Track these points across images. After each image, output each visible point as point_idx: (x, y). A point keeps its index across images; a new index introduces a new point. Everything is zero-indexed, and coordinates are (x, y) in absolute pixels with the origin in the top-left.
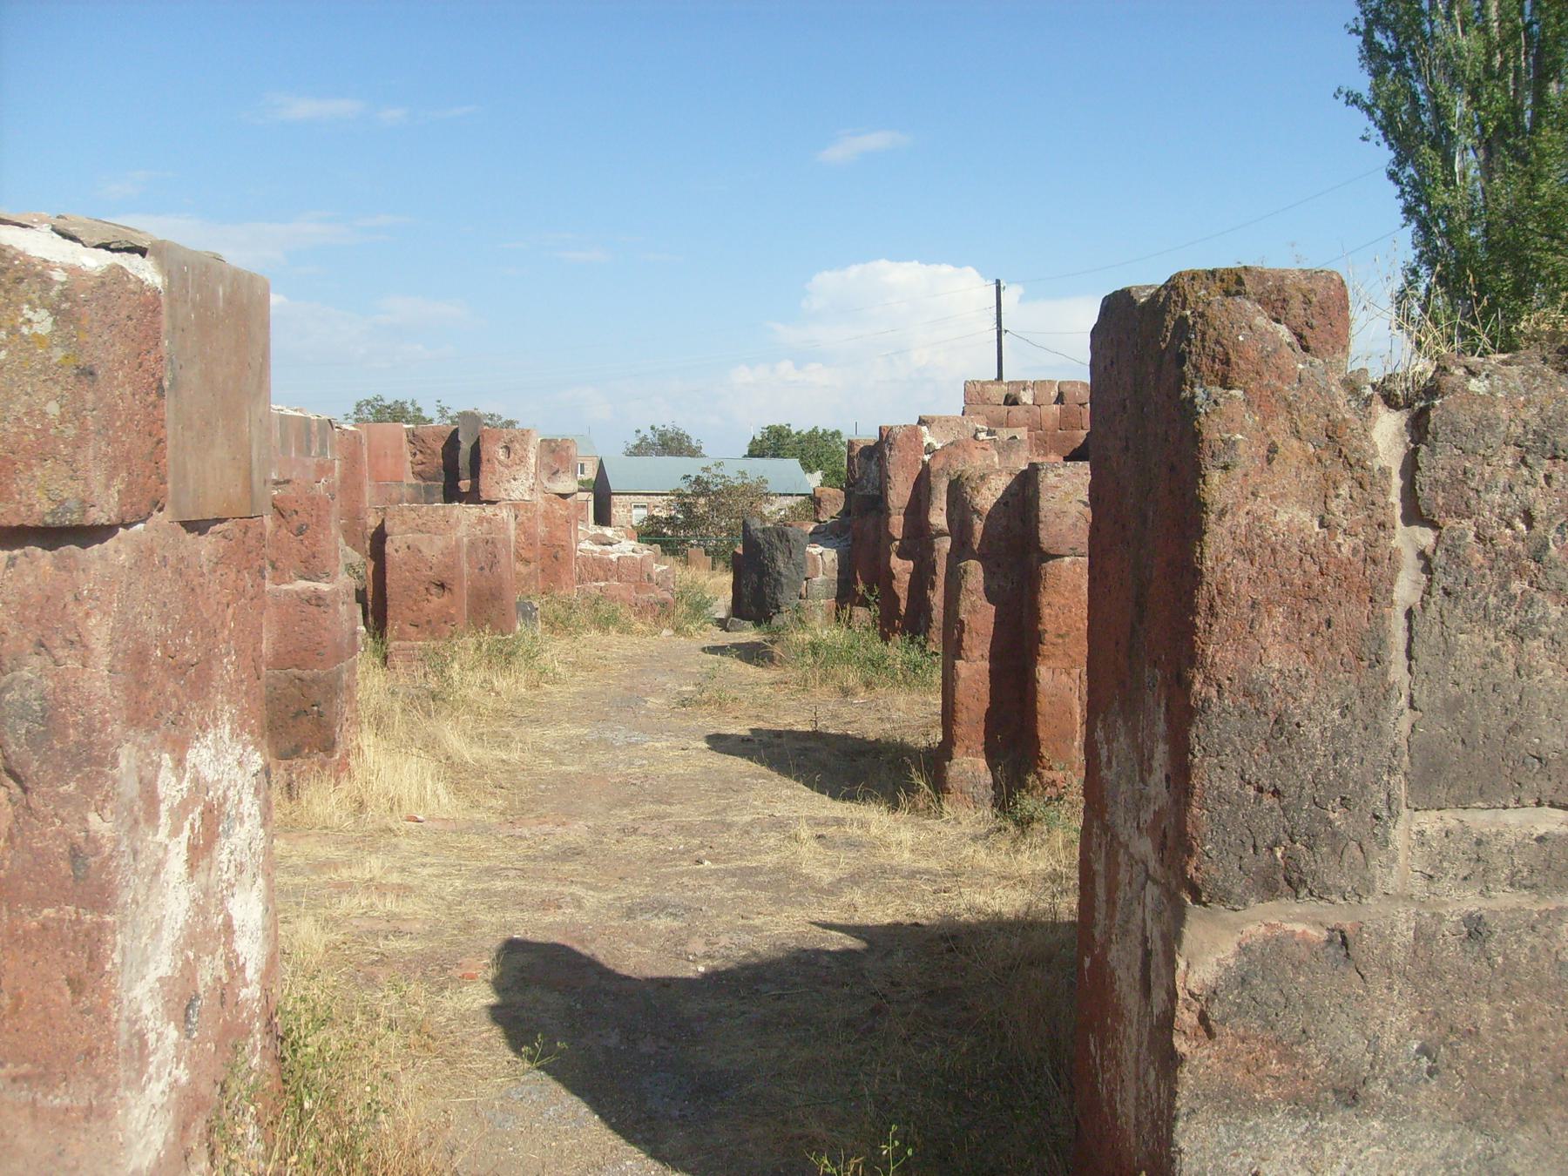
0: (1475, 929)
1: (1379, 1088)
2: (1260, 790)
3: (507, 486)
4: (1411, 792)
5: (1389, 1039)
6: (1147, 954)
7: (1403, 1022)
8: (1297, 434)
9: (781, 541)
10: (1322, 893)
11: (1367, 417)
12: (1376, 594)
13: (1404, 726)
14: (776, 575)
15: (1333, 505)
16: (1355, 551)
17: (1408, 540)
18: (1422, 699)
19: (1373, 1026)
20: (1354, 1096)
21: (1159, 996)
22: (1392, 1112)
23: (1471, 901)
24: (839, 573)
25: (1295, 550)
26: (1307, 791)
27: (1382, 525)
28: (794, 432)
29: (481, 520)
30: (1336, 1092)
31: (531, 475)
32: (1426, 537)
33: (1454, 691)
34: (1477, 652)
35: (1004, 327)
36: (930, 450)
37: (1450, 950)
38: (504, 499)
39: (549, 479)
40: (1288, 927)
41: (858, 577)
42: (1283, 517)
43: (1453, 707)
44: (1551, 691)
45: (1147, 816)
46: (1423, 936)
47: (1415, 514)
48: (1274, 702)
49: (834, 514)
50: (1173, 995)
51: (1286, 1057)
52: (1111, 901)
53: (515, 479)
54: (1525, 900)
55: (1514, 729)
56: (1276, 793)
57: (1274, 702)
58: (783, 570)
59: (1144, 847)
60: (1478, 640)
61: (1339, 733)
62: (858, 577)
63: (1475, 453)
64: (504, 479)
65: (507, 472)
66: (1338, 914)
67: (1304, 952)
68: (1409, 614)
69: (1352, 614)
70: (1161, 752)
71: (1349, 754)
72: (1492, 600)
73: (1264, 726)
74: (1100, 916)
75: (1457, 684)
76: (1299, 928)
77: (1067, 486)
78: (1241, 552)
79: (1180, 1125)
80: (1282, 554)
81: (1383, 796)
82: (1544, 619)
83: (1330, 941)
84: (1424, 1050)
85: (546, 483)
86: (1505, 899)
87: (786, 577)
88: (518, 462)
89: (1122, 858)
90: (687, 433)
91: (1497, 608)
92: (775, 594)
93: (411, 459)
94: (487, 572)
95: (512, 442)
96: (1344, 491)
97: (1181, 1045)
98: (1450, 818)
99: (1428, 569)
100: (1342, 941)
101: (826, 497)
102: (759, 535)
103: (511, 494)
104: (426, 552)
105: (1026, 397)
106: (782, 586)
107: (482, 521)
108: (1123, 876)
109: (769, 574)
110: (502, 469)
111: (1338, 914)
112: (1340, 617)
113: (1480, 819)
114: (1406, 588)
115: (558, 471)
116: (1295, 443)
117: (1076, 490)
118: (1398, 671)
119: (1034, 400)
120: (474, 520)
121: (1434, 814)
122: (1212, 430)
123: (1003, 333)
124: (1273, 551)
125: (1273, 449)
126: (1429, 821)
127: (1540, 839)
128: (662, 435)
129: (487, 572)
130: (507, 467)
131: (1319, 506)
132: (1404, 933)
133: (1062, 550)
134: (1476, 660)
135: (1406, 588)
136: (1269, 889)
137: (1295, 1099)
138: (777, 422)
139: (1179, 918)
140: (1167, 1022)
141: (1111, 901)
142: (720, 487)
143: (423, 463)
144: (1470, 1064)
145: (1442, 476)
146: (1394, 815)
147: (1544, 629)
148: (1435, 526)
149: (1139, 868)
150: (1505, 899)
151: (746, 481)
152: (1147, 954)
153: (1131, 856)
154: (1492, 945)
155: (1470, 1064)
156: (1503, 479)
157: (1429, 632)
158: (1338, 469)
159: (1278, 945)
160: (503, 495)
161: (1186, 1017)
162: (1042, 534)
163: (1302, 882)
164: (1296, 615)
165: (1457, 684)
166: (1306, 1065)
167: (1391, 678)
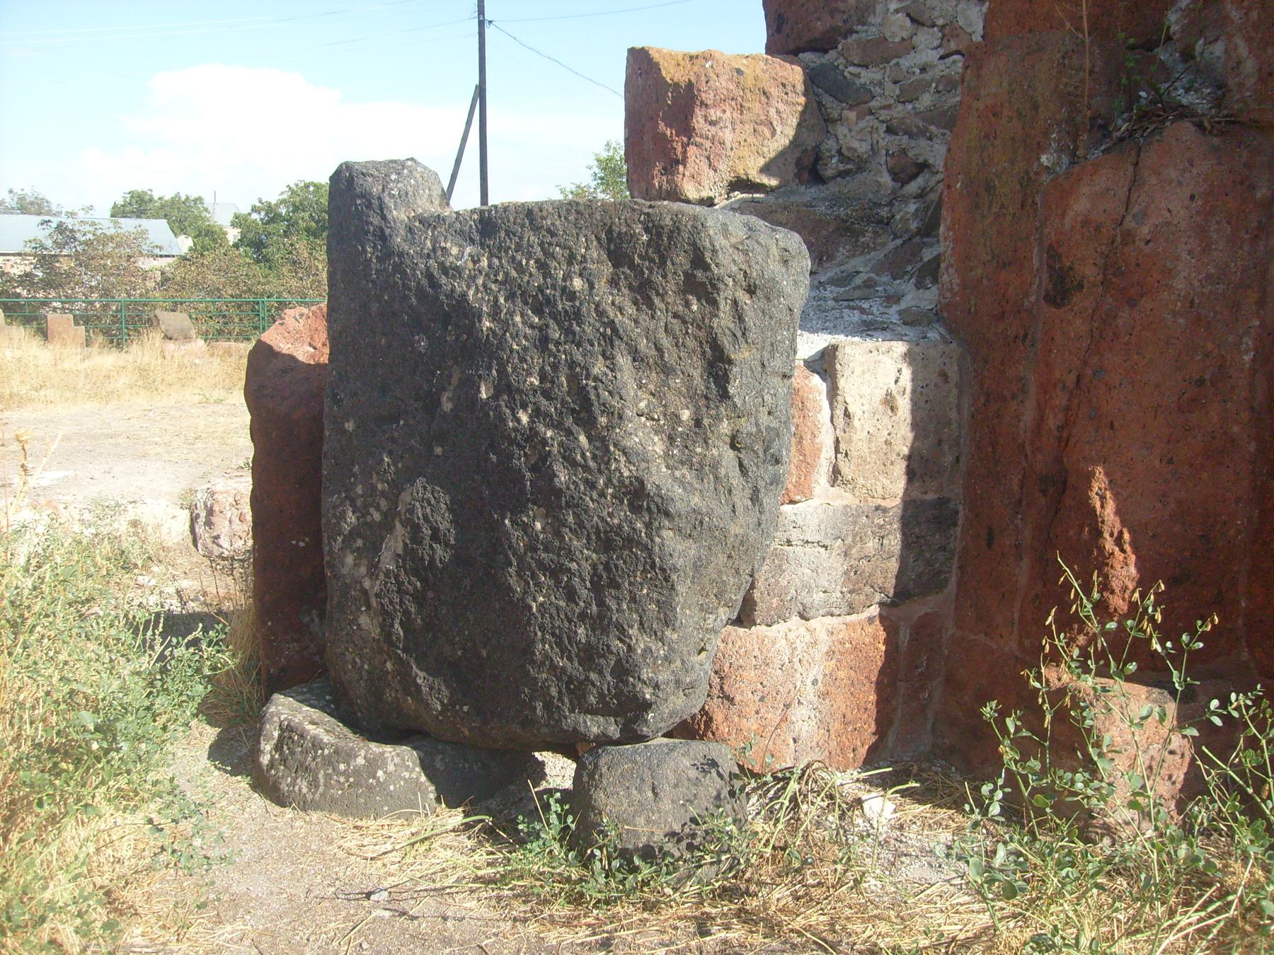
9: (644, 293)
14: (620, 516)
24: (917, 468)
28: (156, 198)
35: (488, 16)
41: (1109, 513)
49: (752, 168)
58: (660, 477)
62: (1109, 513)
87: (698, 525)
90: (47, 198)
92: (601, 623)
101: (723, 84)
102: (459, 253)
106: (662, 576)
109: (551, 499)
123: (486, 24)
128: (22, 199)
138: (140, 187)
142: (90, 236)
151: (119, 231)
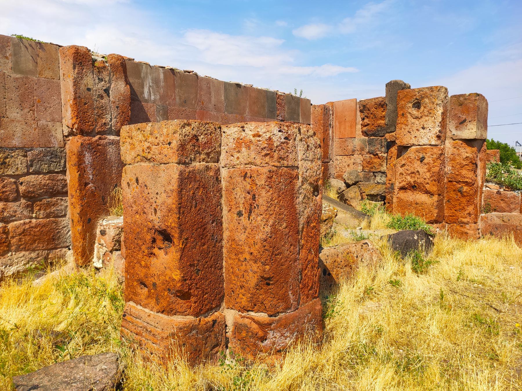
3: (417, 134)
31: (438, 123)
38: (414, 145)
39: (457, 128)
53: (423, 128)
64: (415, 129)
65: (417, 122)
85: (454, 132)
88: (426, 114)
93: (361, 122)
95: (423, 98)
103: (420, 140)
107: (241, 144)
110: (413, 120)
115: (465, 121)
130: (417, 118)
143: (368, 125)
160: (414, 141)
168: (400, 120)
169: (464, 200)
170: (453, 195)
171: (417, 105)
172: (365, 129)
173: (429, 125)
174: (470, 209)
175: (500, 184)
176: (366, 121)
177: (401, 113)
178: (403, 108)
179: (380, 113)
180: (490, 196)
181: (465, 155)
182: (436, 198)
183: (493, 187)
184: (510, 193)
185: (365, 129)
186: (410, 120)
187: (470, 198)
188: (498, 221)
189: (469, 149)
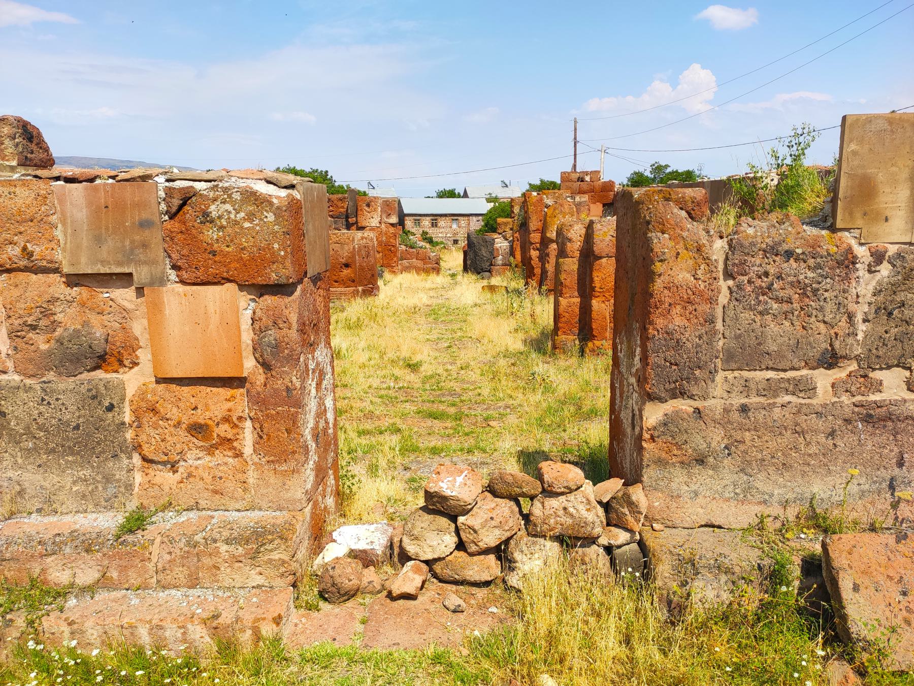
0: (744, 409)
1: (711, 459)
2: (671, 364)
4: (722, 364)
5: (714, 444)
6: (634, 415)
7: (719, 439)
8: (687, 249)
10: (691, 397)
11: (711, 242)
12: (712, 301)
13: (721, 343)
15: (698, 272)
16: (705, 287)
17: (724, 285)
18: (727, 334)
19: (709, 440)
20: (703, 461)
21: (637, 429)
22: (714, 468)
23: (744, 401)
25: (684, 287)
26: (687, 364)
27: (715, 279)
29: (362, 238)
30: (696, 460)
32: (730, 283)
33: (739, 332)
34: (747, 320)
36: (547, 207)
37: (735, 416)
39: (387, 218)
40: (680, 407)
42: (681, 276)
43: (738, 337)
44: (773, 332)
45: (634, 370)
46: (726, 411)
47: (728, 275)
48: (676, 336)
50: (642, 428)
51: (680, 448)
52: (621, 397)
54: (762, 400)
55: (760, 344)
56: (676, 365)
57: (676, 336)
59: (633, 380)
60: (747, 316)
61: (698, 346)
63: (749, 254)
66: (698, 404)
67: (686, 416)
68: (724, 307)
69: (704, 308)
70: (638, 350)
71: (702, 352)
72: (753, 302)
73: (673, 343)
74: (618, 402)
75: (739, 329)
76: (684, 407)
77: (605, 229)
78: (666, 288)
79: (644, 470)
80: (680, 288)
81: (713, 366)
82: (771, 308)
83: (694, 412)
84: (726, 447)
86: (754, 400)
89: (625, 383)
91: (754, 305)
94: (365, 259)
96: (702, 267)
97: (644, 444)
98: (736, 373)
99: (731, 293)
100: (698, 411)
104: (340, 252)
105: (587, 178)
108: (625, 389)
111: (698, 404)
112: (699, 308)
113: (746, 374)
114: (723, 298)
116: (685, 251)
117: (609, 231)
118: (719, 325)
119: (591, 178)
120: (360, 238)
121: (730, 372)
122: (657, 248)
124: (677, 287)
125: (678, 254)
126: (730, 375)
127: (768, 380)
129: (365, 259)
131: (694, 272)
132: (720, 410)
133: (604, 254)
134: (746, 322)
135: (723, 298)
136: (674, 397)
137: (682, 463)
139: (644, 404)
140: (640, 438)
141: (621, 397)
144: (742, 452)
145: (737, 261)
146: (716, 371)
147: (771, 311)
148: (734, 279)
149: (631, 387)
150: (754, 400)
152: (634, 415)
153: (628, 383)
154: (750, 414)
155: (742, 452)
156: (758, 262)
157: (731, 313)
158: (700, 261)
159: (677, 412)
160: (368, 224)
161: (646, 436)
162: (595, 249)
163: (685, 393)
164: (685, 308)
165: (739, 329)
166: (686, 451)
167: (717, 328)
168: (359, 212)
169: (392, 255)
170: (387, 252)
171: (368, 205)
172: (331, 213)
173: (375, 216)
174: (395, 259)
175: (406, 246)
176: (331, 208)
177: (359, 209)
178: (360, 206)
179: (340, 204)
180: (402, 252)
181: (391, 231)
182: (381, 254)
183: (403, 247)
184: (411, 250)
185: (331, 213)
186: (365, 212)
187: (395, 253)
188: (407, 264)
189: (393, 228)
